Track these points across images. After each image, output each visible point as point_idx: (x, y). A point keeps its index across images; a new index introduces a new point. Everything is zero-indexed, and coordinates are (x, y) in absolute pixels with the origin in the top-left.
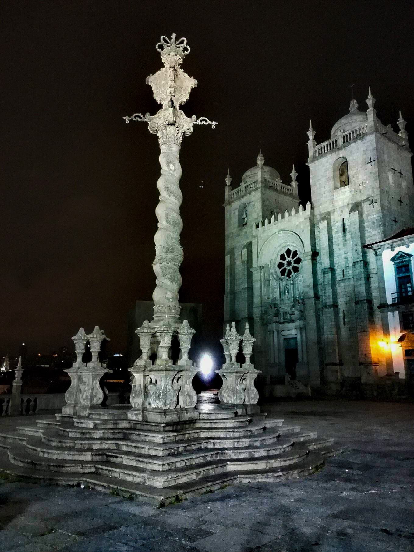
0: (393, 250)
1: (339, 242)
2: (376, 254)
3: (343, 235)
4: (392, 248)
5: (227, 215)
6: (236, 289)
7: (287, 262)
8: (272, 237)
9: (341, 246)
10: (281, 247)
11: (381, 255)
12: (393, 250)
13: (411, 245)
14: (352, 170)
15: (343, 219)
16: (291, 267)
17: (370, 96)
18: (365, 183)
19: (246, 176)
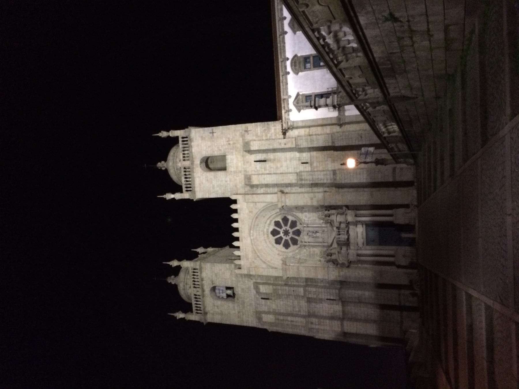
0: (291, 110)
1: (275, 167)
2: (292, 126)
3: (269, 162)
4: (289, 111)
5: (217, 319)
6: (304, 314)
7: (284, 235)
8: (255, 245)
9: (279, 165)
10: (267, 241)
11: (293, 122)
12: (291, 110)
13: (289, 94)
14: (214, 152)
15: (255, 161)
16: (291, 231)
17: (160, 134)
18: (229, 138)
19: (184, 289)
